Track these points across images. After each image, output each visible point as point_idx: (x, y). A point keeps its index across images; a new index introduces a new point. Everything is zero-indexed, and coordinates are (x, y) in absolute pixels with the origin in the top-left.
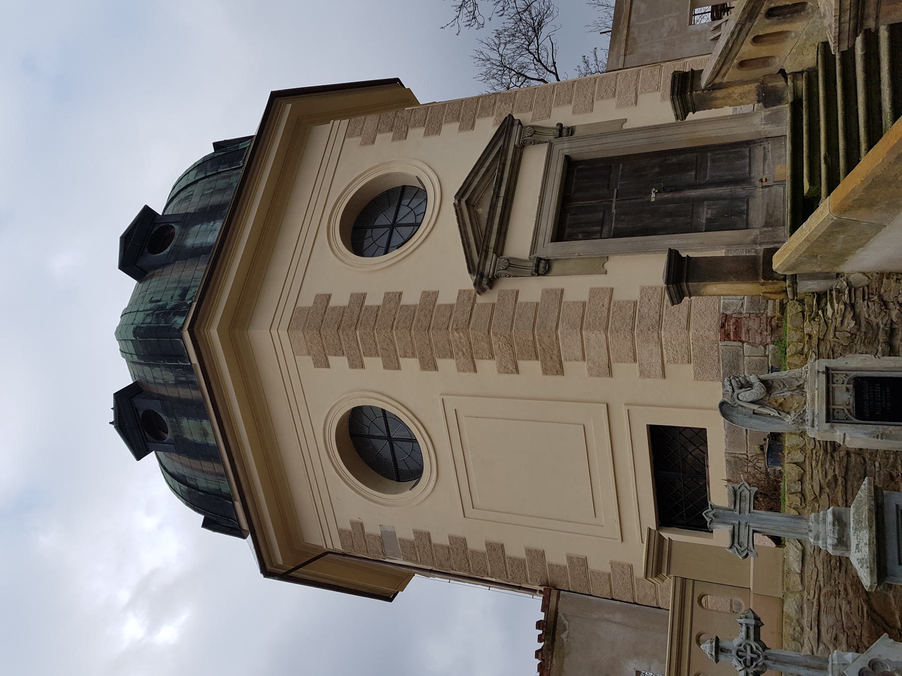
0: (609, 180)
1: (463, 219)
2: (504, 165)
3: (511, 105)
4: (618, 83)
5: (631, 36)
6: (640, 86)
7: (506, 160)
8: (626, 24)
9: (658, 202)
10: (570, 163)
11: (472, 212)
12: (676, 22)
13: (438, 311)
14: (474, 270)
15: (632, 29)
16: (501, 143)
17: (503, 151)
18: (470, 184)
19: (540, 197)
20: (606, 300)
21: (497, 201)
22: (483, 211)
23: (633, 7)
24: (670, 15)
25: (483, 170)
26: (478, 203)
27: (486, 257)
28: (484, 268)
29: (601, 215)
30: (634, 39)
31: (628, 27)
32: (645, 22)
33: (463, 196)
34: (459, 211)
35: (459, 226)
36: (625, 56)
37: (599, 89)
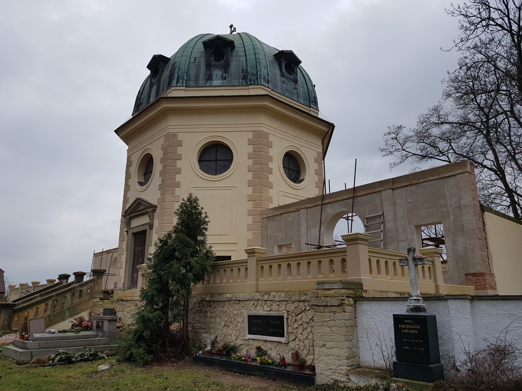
1: (135, 203)
5: (277, 217)
8: (282, 212)
12: (279, 238)
15: (280, 216)
17: (145, 209)
20: (122, 254)
21: (137, 212)
23: (291, 213)
24: (284, 234)
27: (128, 215)
28: (127, 216)
30: (275, 219)
31: (281, 214)
32: (282, 223)
36: (267, 217)
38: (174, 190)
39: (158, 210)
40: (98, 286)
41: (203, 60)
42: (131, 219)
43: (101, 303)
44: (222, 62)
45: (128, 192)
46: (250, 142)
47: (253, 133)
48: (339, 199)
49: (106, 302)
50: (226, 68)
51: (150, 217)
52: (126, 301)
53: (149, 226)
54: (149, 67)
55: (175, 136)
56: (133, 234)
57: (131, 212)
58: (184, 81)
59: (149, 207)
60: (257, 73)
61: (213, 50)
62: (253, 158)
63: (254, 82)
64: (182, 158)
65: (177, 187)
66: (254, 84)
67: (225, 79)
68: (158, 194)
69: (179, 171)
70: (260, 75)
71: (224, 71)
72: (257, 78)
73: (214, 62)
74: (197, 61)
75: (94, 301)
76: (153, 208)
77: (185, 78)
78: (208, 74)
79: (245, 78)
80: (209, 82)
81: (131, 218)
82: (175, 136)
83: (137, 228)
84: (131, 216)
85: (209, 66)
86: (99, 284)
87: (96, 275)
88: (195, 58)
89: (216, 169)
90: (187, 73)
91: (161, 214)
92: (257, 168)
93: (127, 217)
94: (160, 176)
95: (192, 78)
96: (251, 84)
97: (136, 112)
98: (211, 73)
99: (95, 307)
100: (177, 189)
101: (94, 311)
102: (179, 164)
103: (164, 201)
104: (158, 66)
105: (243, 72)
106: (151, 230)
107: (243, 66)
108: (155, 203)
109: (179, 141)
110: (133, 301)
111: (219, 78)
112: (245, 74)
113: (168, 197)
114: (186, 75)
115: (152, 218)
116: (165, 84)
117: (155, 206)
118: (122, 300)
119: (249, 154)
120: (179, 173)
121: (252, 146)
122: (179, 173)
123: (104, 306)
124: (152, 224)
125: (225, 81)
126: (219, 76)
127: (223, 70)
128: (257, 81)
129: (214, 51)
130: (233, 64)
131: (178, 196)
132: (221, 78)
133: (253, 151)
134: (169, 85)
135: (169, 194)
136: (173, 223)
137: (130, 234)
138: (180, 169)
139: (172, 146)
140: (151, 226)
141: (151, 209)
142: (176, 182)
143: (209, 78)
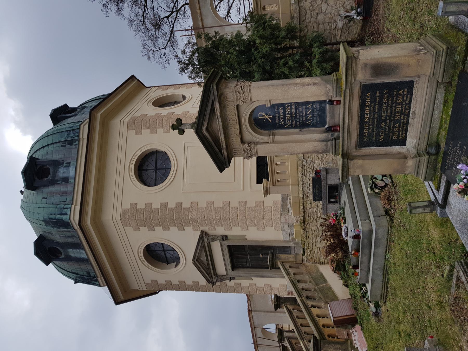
0: (245, 249)
2: (206, 250)
3: (197, 223)
4: (239, 221)
6: (248, 224)
7: (206, 249)
9: (263, 258)
10: (229, 247)
11: (199, 261)
13: (201, 287)
14: (210, 281)
16: (201, 242)
17: (204, 247)
18: (195, 256)
19: (223, 259)
20: (255, 287)
22: (204, 258)
25: (198, 251)
26: (200, 256)
27: (212, 278)
29: (245, 260)
33: (194, 259)
34: (196, 265)
35: (199, 270)
37: (232, 222)
38: (184, 209)
39: (206, 229)
40: (288, 258)
41: (46, 190)
42: (216, 274)
43: (309, 251)
44: (51, 168)
45: (187, 283)
46: (139, 132)
47: (130, 130)
48: (198, 7)
49: (308, 246)
50: (57, 164)
51: (213, 240)
52: (304, 212)
53: (223, 240)
54: (47, 264)
55: (124, 212)
56: (233, 270)
57: (209, 275)
58: (66, 206)
59: (203, 241)
60: (67, 131)
61: (36, 178)
62: (156, 128)
63: (76, 133)
64: (151, 202)
65: (182, 207)
66: (79, 132)
67: (69, 163)
68: (189, 229)
69: (164, 205)
70: (70, 127)
71: (60, 165)
72: (73, 130)
73: (50, 177)
74: (45, 196)
75: (306, 260)
76: (204, 235)
77: (62, 206)
78: (61, 182)
79: (71, 143)
80: (70, 181)
81: (215, 274)
82: (124, 212)
83: (226, 261)
84: (213, 274)
85: (54, 182)
86: (287, 258)
87: (276, 261)
88: (43, 198)
89: (165, 169)
90: (57, 205)
91: (211, 223)
92: (167, 123)
93: (214, 279)
94: (169, 229)
95: (64, 198)
96: (78, 136)
97: (97, 280)
98: (61, 179)
99: (313, 257)
100: (184, 206)
101: (318, 259)
102: (156, 206)
103: (196, 219)
104: (48, 248)
105: (65, 146)
106: (229, 238)
107: (59, 147)
108: (199, 233)
109: (131, 207)
110: (305, 197)
111: (67, 169)
112: (67, 143)
113: (192, 215)
114: (59, 206)
115: (214, 238)
116: (68, 234)
117: (201, 233)
118: (304, 222)
119: (151, 133)
120: (166, 204)
121: (143, 130)
122: (166, 204)
123: (311, 247)
124: (221, 236)
125: (71, 163)
126: (65, 170)
127: (60, 166)
128: (76, 130)
129: (37, 177)
130: (55, 157)
131: (191, 204)
132: (67, 168)
133: (149, 128)
134: (67, 225)
135: (189, 214)
136: (221, 208)
137: (232, 274)
138: (162, 204)
139: (136, 215)
140: (224, 238)
141: (204, 237)
142: (176, 207)
143: (66, 180)
